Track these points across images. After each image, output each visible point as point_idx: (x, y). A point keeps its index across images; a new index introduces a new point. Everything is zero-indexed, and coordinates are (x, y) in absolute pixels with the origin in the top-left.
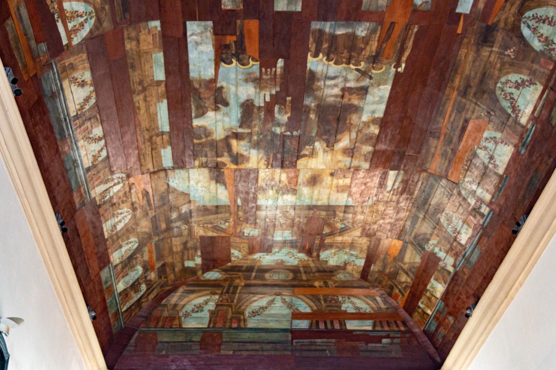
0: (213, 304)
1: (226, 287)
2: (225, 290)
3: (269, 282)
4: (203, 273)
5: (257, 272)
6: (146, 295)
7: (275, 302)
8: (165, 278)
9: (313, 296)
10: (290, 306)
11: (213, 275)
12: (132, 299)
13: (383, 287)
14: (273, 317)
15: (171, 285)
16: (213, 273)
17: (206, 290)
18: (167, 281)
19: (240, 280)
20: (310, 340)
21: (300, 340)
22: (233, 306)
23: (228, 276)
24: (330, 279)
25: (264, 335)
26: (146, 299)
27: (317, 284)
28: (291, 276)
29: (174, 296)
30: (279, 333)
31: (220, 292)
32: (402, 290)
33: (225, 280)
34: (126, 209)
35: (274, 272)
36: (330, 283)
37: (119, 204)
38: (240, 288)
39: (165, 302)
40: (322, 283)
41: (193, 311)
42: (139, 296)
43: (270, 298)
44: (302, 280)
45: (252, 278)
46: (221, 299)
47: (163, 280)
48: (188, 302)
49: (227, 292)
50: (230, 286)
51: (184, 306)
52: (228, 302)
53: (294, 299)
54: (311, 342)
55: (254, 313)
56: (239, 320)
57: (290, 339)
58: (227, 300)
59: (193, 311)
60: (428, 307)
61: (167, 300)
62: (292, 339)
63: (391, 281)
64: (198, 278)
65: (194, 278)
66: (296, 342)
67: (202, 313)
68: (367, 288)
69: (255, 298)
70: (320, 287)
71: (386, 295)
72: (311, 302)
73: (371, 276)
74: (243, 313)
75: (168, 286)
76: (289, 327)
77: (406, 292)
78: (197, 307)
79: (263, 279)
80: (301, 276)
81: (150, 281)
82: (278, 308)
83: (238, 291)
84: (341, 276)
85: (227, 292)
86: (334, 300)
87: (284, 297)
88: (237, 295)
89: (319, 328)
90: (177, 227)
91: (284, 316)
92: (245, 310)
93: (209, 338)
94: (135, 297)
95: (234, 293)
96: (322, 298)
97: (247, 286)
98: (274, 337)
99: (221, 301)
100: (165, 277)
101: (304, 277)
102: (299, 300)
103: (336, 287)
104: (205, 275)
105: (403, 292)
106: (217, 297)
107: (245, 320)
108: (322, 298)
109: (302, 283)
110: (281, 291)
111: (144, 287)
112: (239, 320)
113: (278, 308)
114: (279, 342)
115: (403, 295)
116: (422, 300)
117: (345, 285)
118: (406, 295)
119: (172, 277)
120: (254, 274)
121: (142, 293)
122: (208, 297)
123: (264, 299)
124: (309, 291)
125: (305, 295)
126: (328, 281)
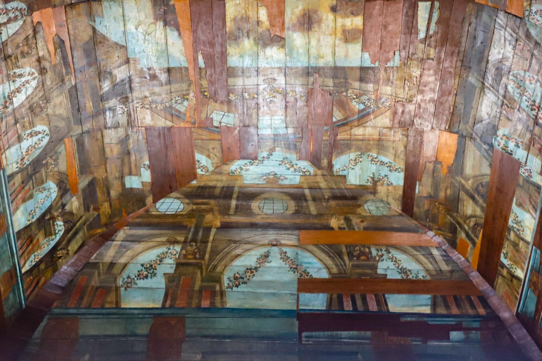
0: (171, 261)
1: (192, 230)
2: (190, 236)
3: (258, 220)
4: (155, 201)
5: (238, 198)
6: (64, 243)
7: (270, 259)
8: (94, 209)
9: (330, 246)
10: (295, 268)
11: (170, 205)
12: (39, 247)
13: (439, 229)
14: (268, 288)
15: (106, 225)
16: (171, 200)
17: (160, 235)
18: (99, 215)
19: (213, 214)
20: (329, 333)
21: (314, 333)
22: (204, 267)
23: (194, 207)
24: (354, 213)
25: (253, 324)
26: (64, 252)
27: (334, 223)
28: (292, 205)
29: (109, 247)
30: (276, 320)
31: (182, 239)
32: (470, 233)
33: (191, 215)
34: (28, 69)
35: (266, 199)
36: (355, 221)
37: (16, 58)
38: (213, 231)
39: (96, 258)
40: (342, 222)
41: (139, 276)
42: (53, 243)
43: (262, 251)
44: (310, 214)
45: (232, 211)
46: (184, 252)
47: (93, 213)
48: (133, 257)
49: (194, 240)
50: (197, 228)
51: (125, 265)
52: (195, 258)
53: (300, 251)
54: (331, 337)
55: (238, 280)
56: (213, 294)
57: (297, 330)
58: (194, 254)
59: (139, 276)
60: (516, 262)
61: (99, 254)
62: (301, 331)
63: (451, 216)
64: (147, 211)
65: (142, 211)
66: (306, 337)
67: (154, 279)
68: (415, 231)
69: (238, 251)
70: (340, 228)
71: (446, 246)
72: (327, 258)
73: (418, 207)
74: (219, 280)
75: (100, 227)
76: (295, 308)
77: (477, 237)
78: (146, 268)
79: (248, 212)
80: (308, 207)
81: (71, 213)
82: (276, 270)
83: (211, 238)
84: (371, 208)
85: (194, 240)
86: (362, 253)
87: (284, 249)
88: (210, 245)
89: (343, 309)
90: (110, 109)
91: (285, 284)
92: (222, 273)
93: (165, 325)
94: (46, 245)
95: (205, 242)
96: (344, 250)
97: (226, 227)
98: (270, 326)
99: (185, 256)
100: (96, 209)
101: (313, 209)
102: (308, 254)
103: (365, 229)
104: (158, 205)
105: (473, 236)
106: (178, 248)
107: (222, 293)
108: (344, 250)
109: (312, 221)
110: (278, 237)
111: (60, 226)
112: (213, 294)
113: (276, 270)
114: (280, 337)
115: (474, 243)
116: (504, 251)
117: (379, 226)
118: (478, 241)
119: (105, 208)
120: (234, 203)
121: (58, 237)
122: (164, 249)
123: (253, 253)
124: (324, 237)
125: (316, 245)
126: (351, 216)
